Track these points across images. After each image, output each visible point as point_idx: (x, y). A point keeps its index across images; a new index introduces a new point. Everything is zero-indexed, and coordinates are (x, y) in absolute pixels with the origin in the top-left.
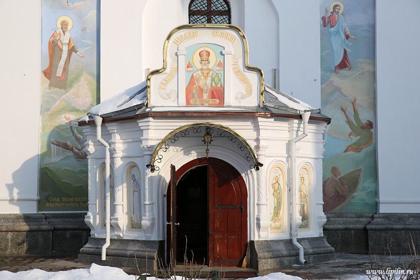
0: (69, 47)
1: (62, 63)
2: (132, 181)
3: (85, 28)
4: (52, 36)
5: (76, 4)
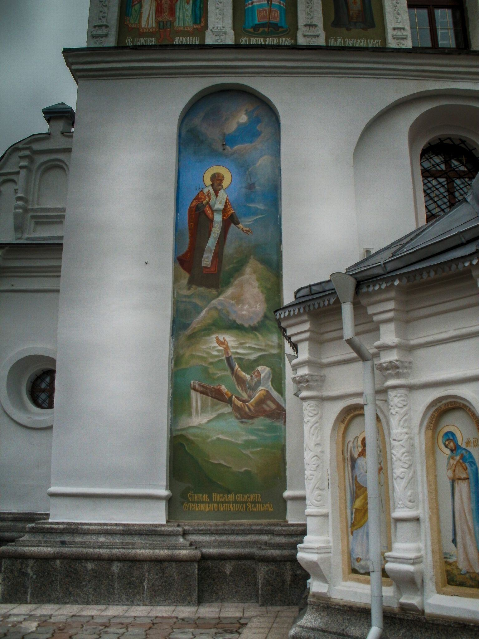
0: (224, 216)
1: (212, 243)
2: (448, 452)
3: (254, 184)
4: (195, 199)
5: (236, 148)
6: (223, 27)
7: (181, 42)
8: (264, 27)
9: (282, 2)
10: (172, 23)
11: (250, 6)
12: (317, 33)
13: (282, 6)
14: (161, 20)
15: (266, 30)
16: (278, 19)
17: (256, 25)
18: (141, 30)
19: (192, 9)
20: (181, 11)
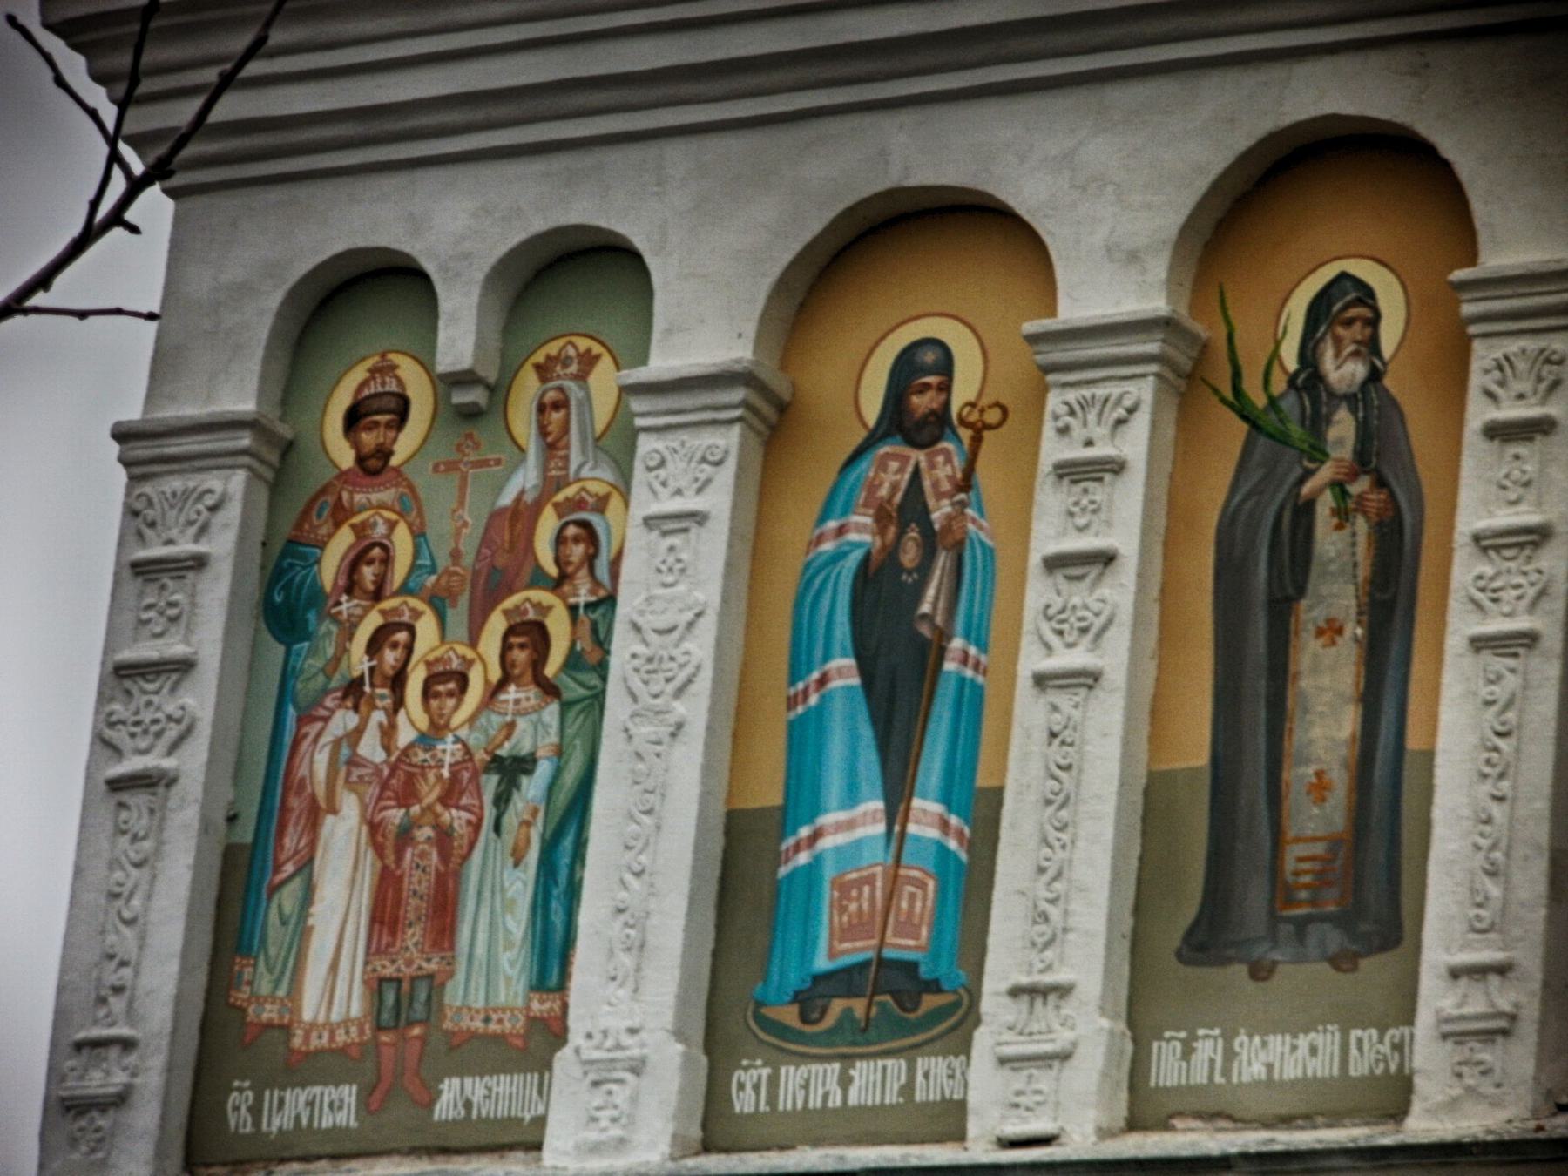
6: (633, 1031)
7: (468, 1105)
8: (851, 993)
9: (954, 820)
10: (435, 984)
11: (803, 858)
12: (1062, 1039)
13: (953, 844)
14: (389, 971)
15: (859, 1006)
16: (924, 932)
17: (818, 978)
18: (297, 1042)
19: (535, 894)
20: (485, 911)
